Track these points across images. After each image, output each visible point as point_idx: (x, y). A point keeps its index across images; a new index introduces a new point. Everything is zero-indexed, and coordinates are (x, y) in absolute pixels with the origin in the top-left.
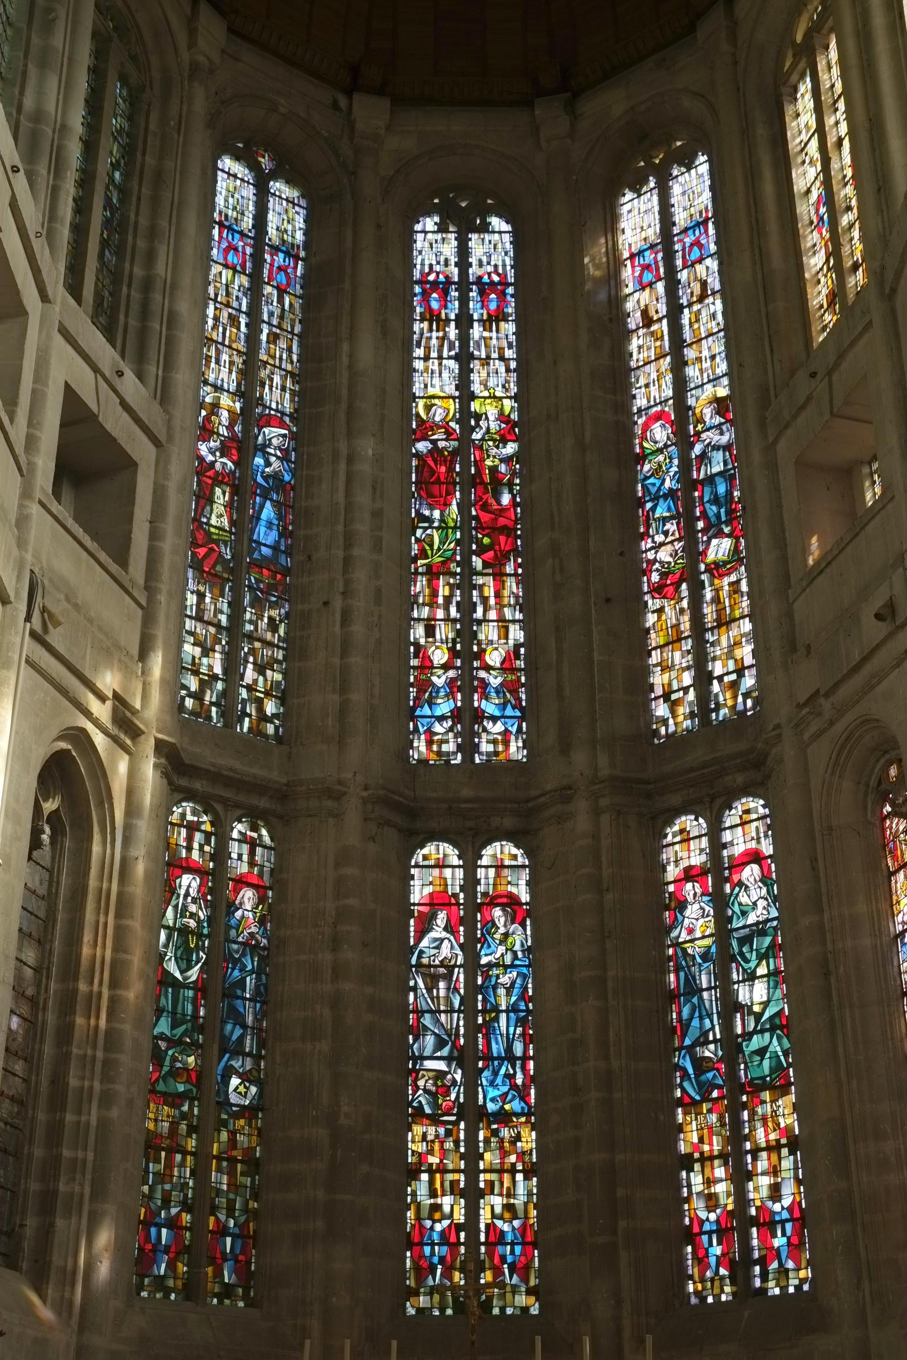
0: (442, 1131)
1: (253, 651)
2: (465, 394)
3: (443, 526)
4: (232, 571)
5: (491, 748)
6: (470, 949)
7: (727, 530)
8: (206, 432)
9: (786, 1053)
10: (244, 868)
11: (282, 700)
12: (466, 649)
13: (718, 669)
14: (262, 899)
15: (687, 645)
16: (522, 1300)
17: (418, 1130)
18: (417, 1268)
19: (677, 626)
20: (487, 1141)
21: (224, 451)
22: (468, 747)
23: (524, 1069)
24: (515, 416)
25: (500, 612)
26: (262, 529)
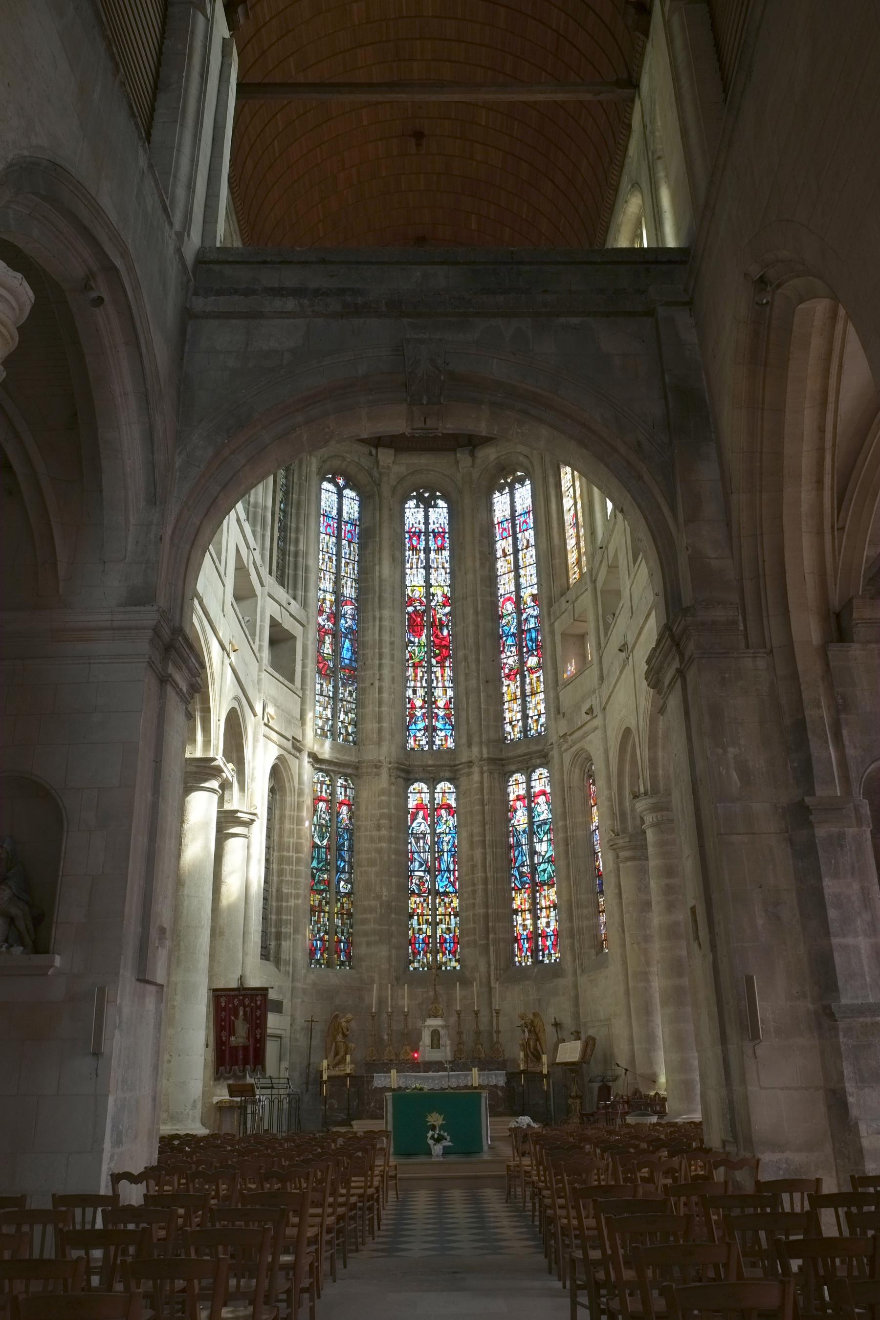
0: (422, 899)
1: (343, 706)
2: (428, 585)
3: (419, 645)
5: (440, 743)
6: (433, 826)
7: (535, 653)
8: (321, 612)
9: (553, 872)
10: (342, 798)
11: (355, 726)
12: (430, 701)
13: (531, 713)
14: (350, 810)
15: (519, 701)
16: (453, 964)
17: (413, 899)
18: (413, 953)
19: (515, 693)
20: (440, 903)
21: (328, 619)
22: (431, 743)
23: (454, 875)
24: (449, 595)
25: (443, 683)
26: (345, 652)
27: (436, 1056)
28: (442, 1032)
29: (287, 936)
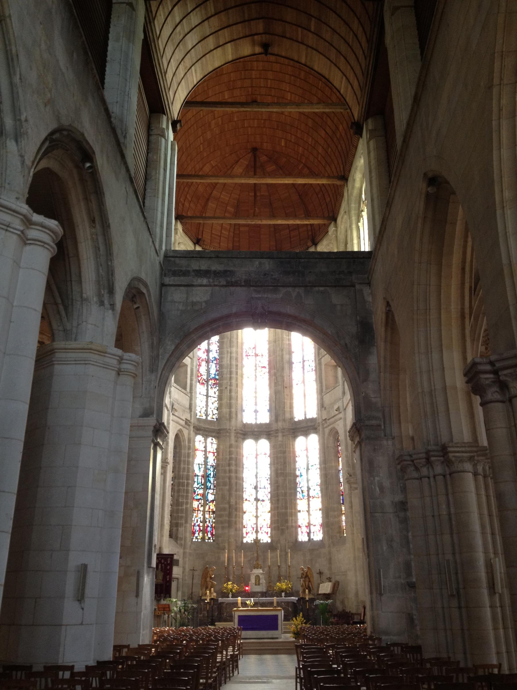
4: (206, 382)
27: (258, 589)
28: (261, 576)
29: (181, 525)
